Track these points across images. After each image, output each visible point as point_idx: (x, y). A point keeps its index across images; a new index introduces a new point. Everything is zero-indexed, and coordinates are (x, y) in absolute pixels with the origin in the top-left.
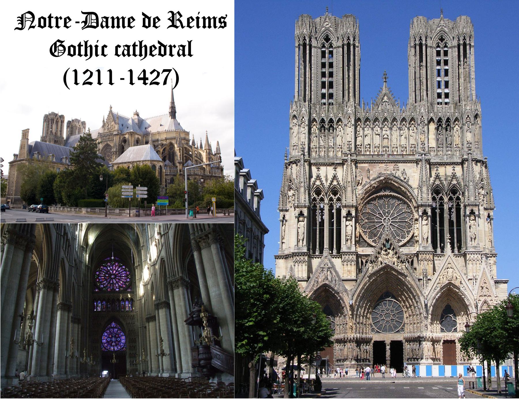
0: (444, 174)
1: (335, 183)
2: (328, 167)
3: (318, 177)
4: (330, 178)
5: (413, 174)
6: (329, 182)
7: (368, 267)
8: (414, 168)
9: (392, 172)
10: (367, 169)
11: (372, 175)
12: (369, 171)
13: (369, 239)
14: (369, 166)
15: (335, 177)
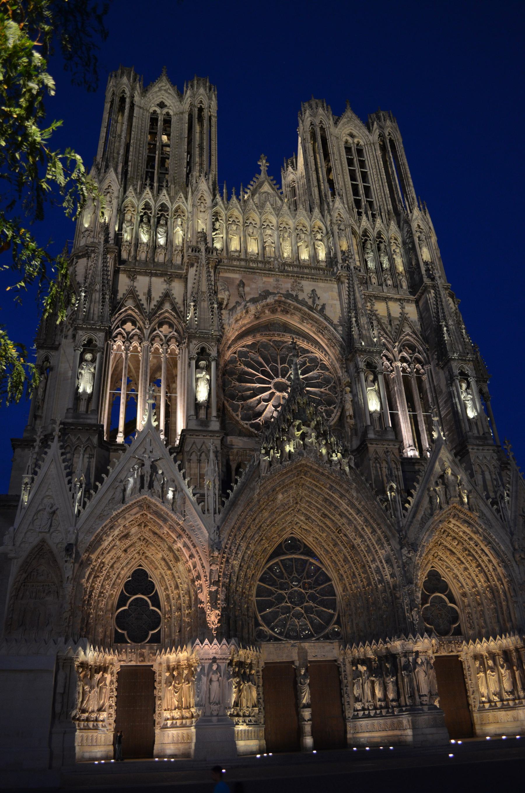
0: (386, 314)
1: (167, 307)
2: (154, 279)
3: (132, 293)
4: (156, 295)
5: (331, 302)
6: (154, 303)
7: (256, 463)
8: (332, 291)
9: (290, 292)
10: (237, 282)
11: (249, 294)
12: (242, 284)
13: (243, 419)
14: (243, 277)
15: (167, 296)
